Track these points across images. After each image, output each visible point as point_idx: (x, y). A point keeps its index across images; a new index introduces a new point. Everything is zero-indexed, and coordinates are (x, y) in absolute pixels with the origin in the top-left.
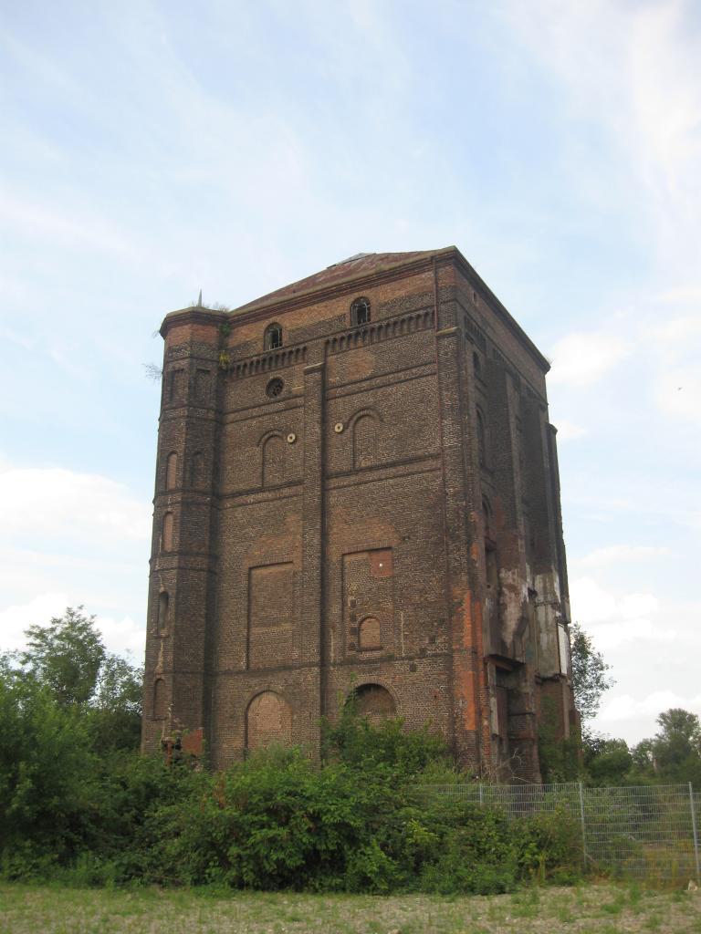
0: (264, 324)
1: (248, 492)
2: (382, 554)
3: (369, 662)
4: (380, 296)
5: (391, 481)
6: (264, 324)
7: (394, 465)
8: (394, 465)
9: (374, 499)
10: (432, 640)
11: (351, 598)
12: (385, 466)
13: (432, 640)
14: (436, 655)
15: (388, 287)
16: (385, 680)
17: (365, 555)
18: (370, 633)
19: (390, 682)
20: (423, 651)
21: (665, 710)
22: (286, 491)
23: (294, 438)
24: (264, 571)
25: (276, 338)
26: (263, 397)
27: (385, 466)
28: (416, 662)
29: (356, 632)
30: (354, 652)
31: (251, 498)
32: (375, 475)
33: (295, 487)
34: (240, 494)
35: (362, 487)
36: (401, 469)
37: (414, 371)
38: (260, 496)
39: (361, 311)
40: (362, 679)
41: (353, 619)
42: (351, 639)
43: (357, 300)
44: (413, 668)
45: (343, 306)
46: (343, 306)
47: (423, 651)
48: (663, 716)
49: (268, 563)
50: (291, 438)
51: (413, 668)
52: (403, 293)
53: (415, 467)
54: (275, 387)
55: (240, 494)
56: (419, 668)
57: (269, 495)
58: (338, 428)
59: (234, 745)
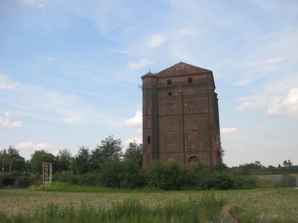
1: (165, 116)
2: (196, 131)
3: (193, 152)
5: (198, 117)
6: (167, 80)
7: (198, 114)
8: (198, 114)
10: (207, 148)
12: (196, 114)
13: (207, 148)
14: (208, 151)
15: (196, 76)
16: (197, 156)
17: (192, 131)
18: (193, 146)
19: (198, 156)
22: (174, 117)
24: (169, 133)
25: (169, 83)
26: (168, 96)
27: (196, 114)
28: (204, 152)
29: (190, 146)
30: (190, 150)
31: (165, 117)
32: (194, 115)
34: (163, 116)
35: (191, 118)
36: (200, 115)
38: (167, 117)
39: (190, 80)
40: (192, 155)
41: (190, 143)
43: (189, 78)
44: (203, 154)
45: (186, 79)
47: (205, 150)
50: (175, 105)
51: (203, 154)
52: (200, 78)
53: (203, 115)
54: (170, 94)
55: (163, 116)
57: (170, 117)
58: (186, 105)
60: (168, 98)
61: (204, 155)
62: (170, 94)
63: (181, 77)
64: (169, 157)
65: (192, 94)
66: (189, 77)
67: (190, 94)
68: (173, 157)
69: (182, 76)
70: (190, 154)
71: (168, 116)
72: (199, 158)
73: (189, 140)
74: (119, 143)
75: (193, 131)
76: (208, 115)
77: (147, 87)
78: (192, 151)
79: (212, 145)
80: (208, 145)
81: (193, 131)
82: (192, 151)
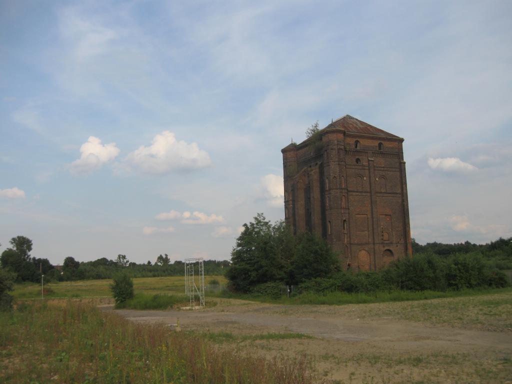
0: (355, 140)
1: (354, 192)
3: (387, 244)
4: (386, 144)
6: (355, 140)
10: (400, 240)
11: (382, 227)
13: (400, 240)
16: (391, 249)
17: (384, 216)
18: (386, 236)
20: (398, 242)
21: (15, 236)
22: (364, 194)
26: (355, 163)
29: (383, 235)
31: (354, 194)
32: (385, 195)
34: (351, 191)
35: (384, 198)
36: (393, 195)
38: (357, 194)
40: (387, 248)
41: (382, 232)
42: (382, 237)
44: (397, 246)
45: (376, 143)
46: (376, 143)
48: (14, 239)
50: (365, 178)
51: (397, 246)
52: (390, 146)
54: (358, 160)
55: (351, 191)
59: (356, 264)
60: (356, 167)
62: (358, 160)
64: (361, 250)
66: (379, 142)
67: (380, 166)
68: (365, 250)
69: (372, 138)
70: (384, 247)
71: (357, 192)
72: (393, 251)
73: (382, 228)
74: (10, 242)
75: (386, 215)
76: (400, 196)
77: (339, 146)
78: (386, 242)
79: (407, 235)
81: (386, 215)
82: (386, 242)
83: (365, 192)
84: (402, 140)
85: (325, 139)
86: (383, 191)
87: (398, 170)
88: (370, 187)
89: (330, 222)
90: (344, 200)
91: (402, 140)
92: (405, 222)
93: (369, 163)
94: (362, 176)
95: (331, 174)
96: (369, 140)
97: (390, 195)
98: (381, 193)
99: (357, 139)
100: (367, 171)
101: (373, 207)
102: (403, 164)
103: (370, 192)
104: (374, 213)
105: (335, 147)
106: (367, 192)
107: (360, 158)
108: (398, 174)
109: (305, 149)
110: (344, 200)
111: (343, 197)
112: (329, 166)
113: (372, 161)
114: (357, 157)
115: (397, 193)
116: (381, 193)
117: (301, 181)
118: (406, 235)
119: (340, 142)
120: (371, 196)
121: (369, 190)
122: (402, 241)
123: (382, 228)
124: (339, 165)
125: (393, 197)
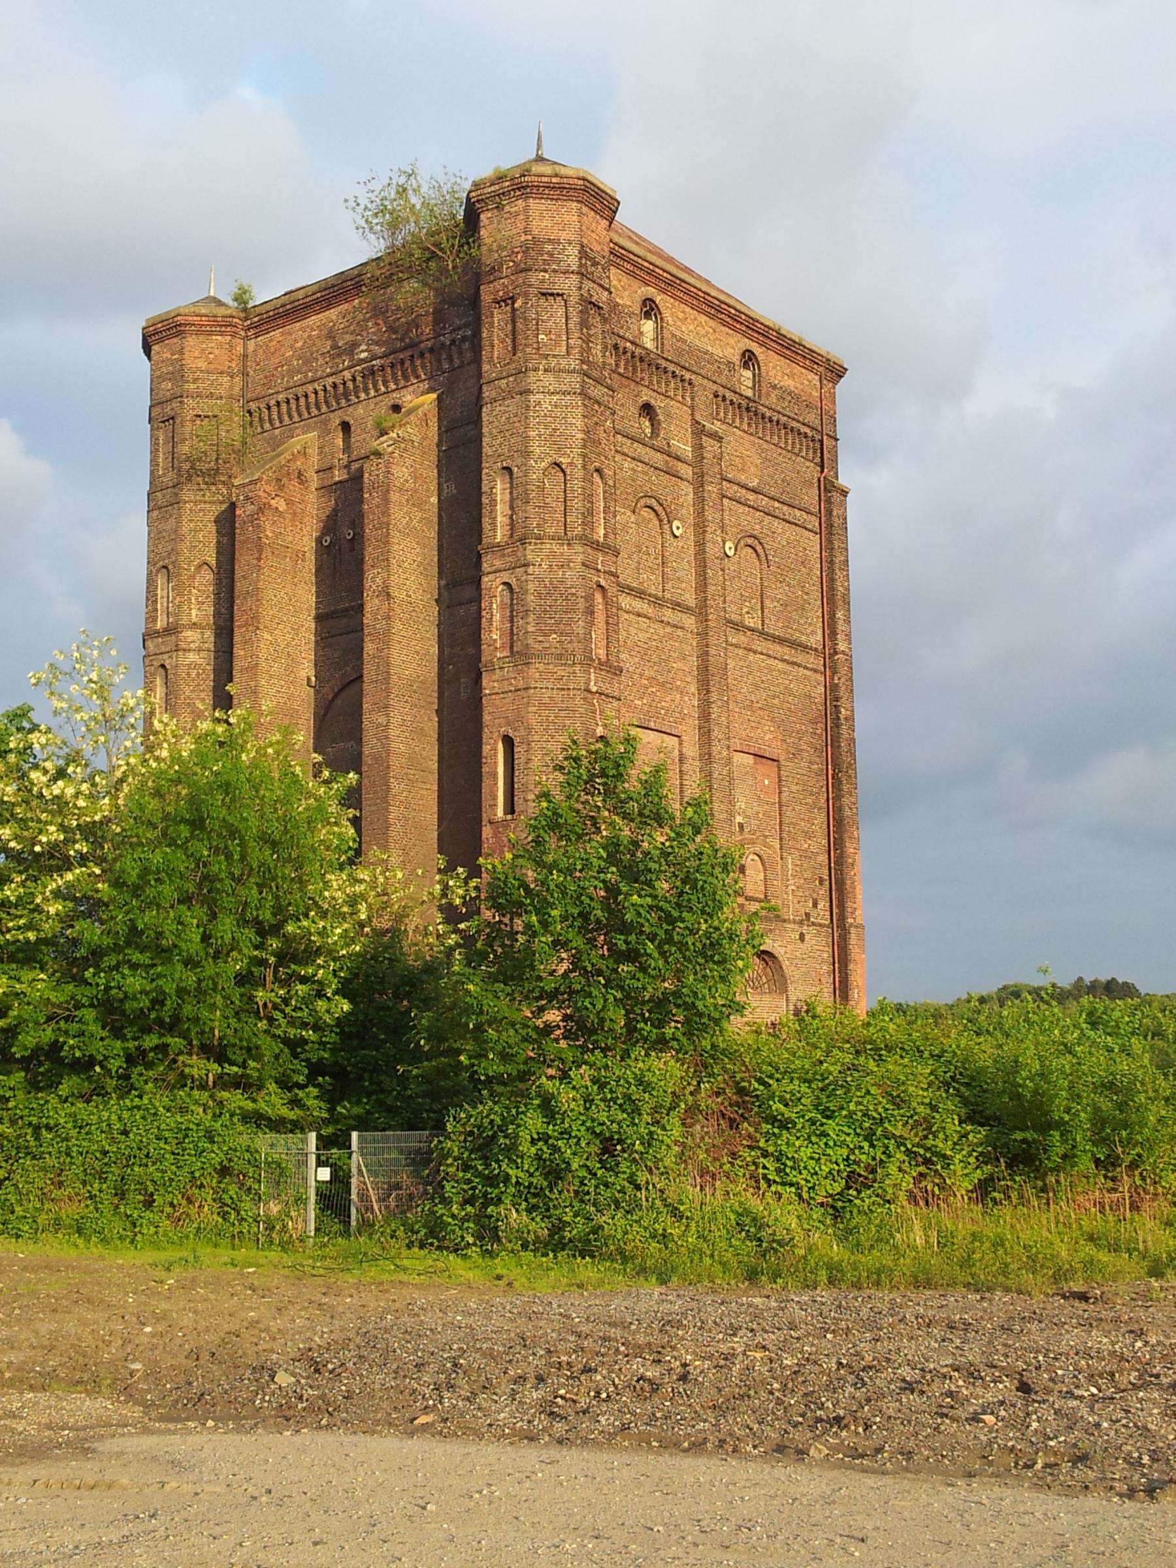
5: (781, 666)
8: (781, 640)
9: (763, 682)
10: (815, 905)
11: (739, 819)
13: (815, 905)
17: (750, 760)
20: (807, 915)
22: (668, 614)
23: (677, 533)
32: (760, 645)
33: (680, 614)
35: (751, 657)
37: (798, 513)
44: (802, 937)
46: (731, 346)
49: (652, 725)
51: (802, 937)
52: (789, 383)
53: (800, 658)
56: (807, 937)
61: (803, 946)
63: (712, 323)
65: (754, 483)
66: (746, 344)
67: (742, 478)
72: (785, 964)
73: (741, 826)
80: (821, 881)
83: (677, 606)
84: (836, 372)
85: (490, 228)
86: (749, 622)
87: (814, 522)
88: (702, 583)
89: (509, 742)
90: (600, 617)
91: (836, 372)
92: (839, 810)
93: (699, 448)
94: (663, 513)
95: (536, 449)
96: (703, 318)
97: (778, 649)
98: (738, 626)
99: (650, 291)
100: (687, 493)
101: (714, 696)
102: (836, 497)
103: (701, 611)
104: (716, 733)
105: (568, 285)
106: (686, 609)
107: (658, 403)
108: (813, 543)
109: (314, 320)
110: (600, 617)
111: (598, 597)
112: (528, 392)
113: (716, 436)
114: (646, 396)
115: (805, 648)
116: (738, 626)
117: (282, 507)
118: (841, 884)
119: (595, 264)
120: (703, 634)
121: (690, 599)
122: (822, 914)
123: (741, 826)
124: (583, 394)
125: (794, 663)
